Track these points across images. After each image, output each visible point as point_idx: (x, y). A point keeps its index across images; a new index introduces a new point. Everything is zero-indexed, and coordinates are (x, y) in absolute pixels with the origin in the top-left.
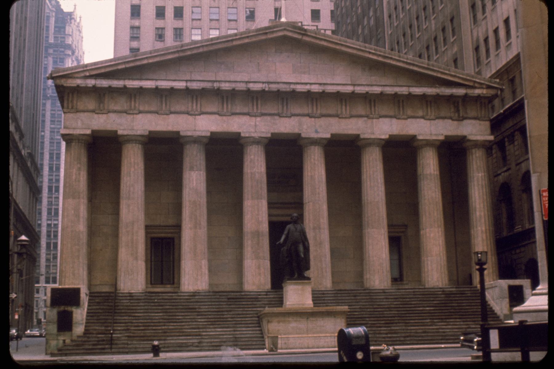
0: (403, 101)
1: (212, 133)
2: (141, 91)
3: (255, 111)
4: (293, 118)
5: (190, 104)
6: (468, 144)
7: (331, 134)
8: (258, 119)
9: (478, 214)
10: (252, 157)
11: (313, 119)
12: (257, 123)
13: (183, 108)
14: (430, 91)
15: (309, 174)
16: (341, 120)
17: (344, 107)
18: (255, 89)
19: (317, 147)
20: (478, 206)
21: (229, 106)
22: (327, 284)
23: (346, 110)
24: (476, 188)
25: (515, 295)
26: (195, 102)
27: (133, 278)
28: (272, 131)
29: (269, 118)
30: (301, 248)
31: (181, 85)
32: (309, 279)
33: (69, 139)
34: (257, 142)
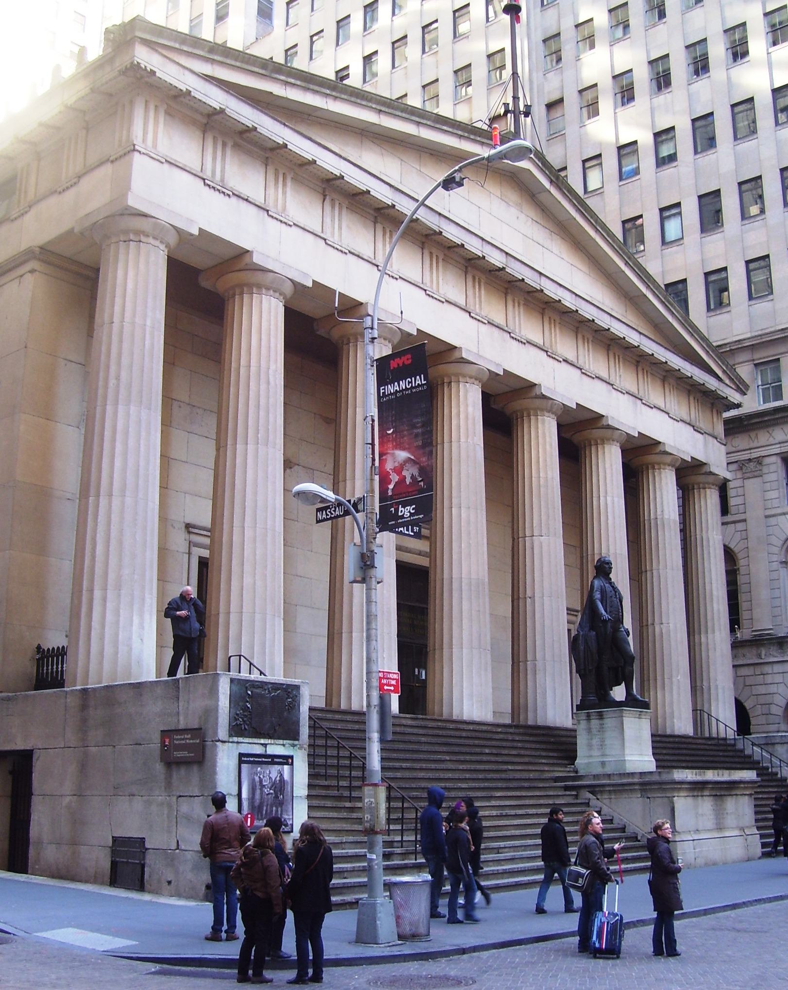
6: (701, 479)
8: (485, 329)
9: (715, 605)
16: (584, 377)
20: (715, 593)
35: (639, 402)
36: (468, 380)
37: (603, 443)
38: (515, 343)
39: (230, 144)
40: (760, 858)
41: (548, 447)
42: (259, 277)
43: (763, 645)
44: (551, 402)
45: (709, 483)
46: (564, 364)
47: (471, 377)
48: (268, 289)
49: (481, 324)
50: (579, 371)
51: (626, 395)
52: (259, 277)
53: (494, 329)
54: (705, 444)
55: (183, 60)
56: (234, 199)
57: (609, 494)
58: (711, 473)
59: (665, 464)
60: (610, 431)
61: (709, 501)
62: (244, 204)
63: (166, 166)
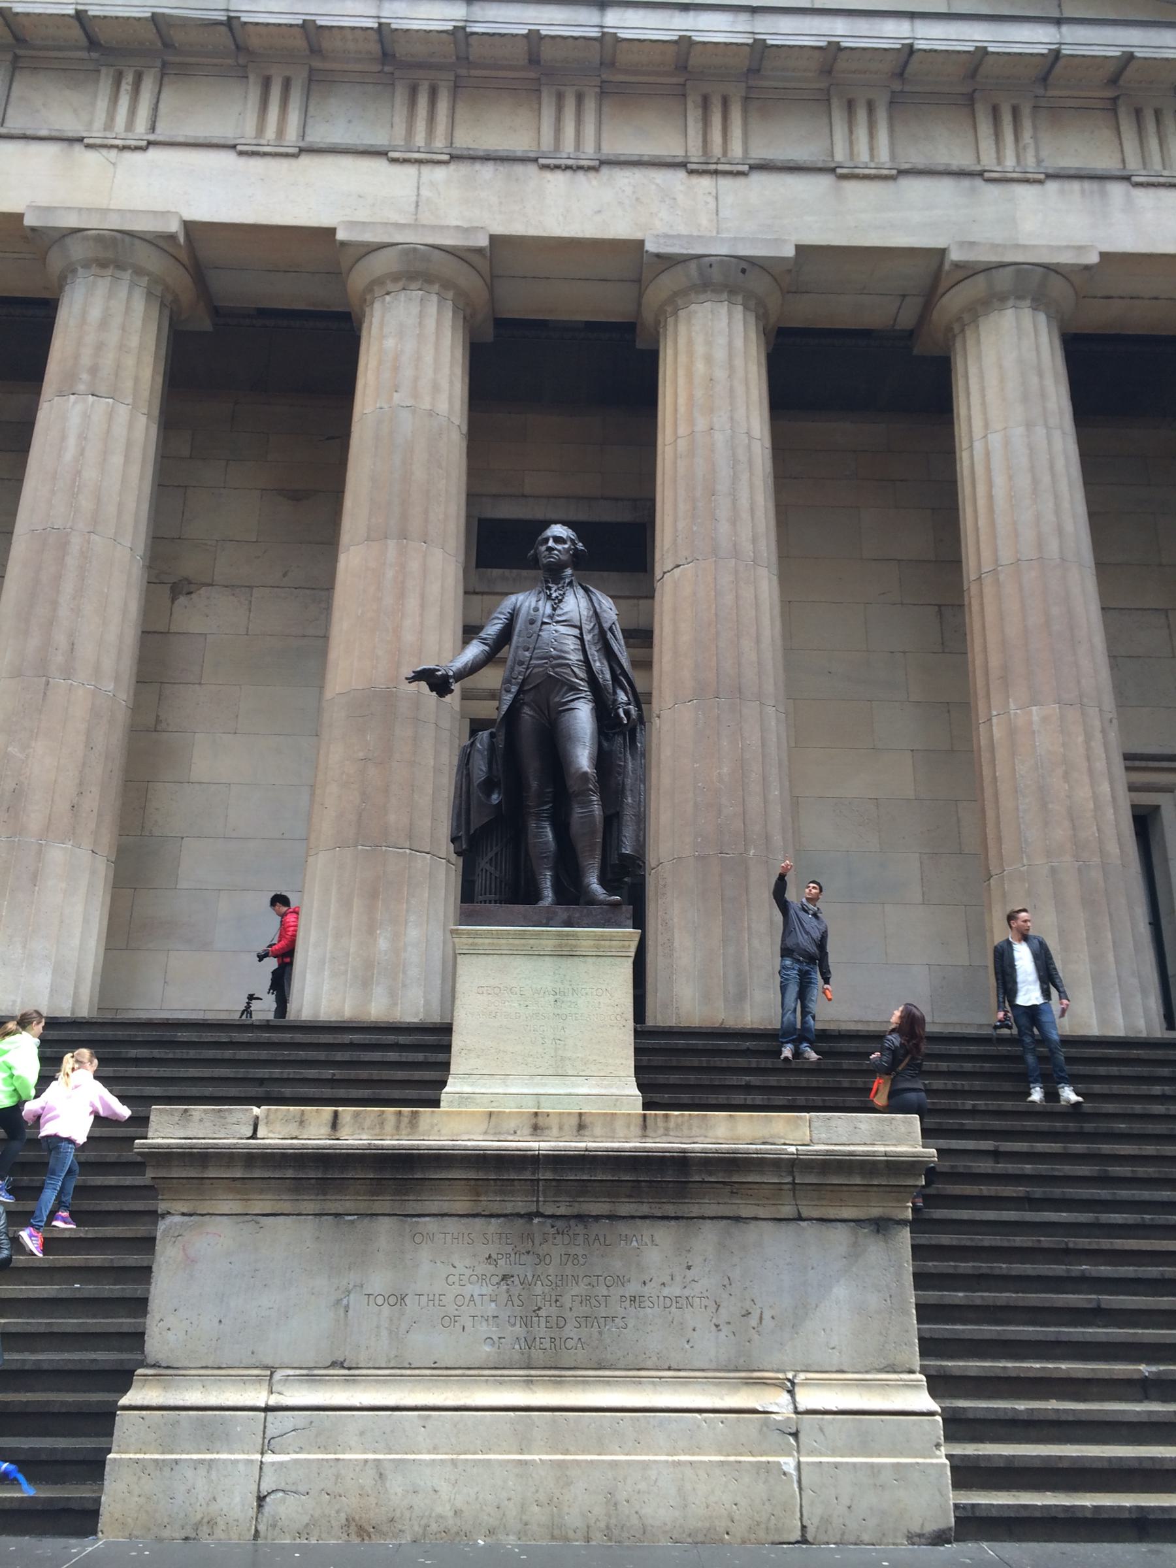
1: (188, 225)
3: (420, 139)
4: (605, 171)
5: (102, 104)
7: (799, 248)
10: (390, 343)
11: (706, 182)
12: (425, 192)
15: (682, 431)
16: (850, 186)
17: (862, 133)
18: (415, 25)
19: (723, 309)
21: (294, 118)
23: (872, 149)
28: (499, 229)
29: (487, 171)
35: (1117, 190)
36: (390, 286)
37: (975, 319)
38: (559, 178)
40: (940, 1538)
41: (700, 367)
44: (693, 265)
46: (757, 178)
47: (396, 277)
49: (426, 170)
51: (1052, 186)
53: (478, 166)
60: (981, 279)
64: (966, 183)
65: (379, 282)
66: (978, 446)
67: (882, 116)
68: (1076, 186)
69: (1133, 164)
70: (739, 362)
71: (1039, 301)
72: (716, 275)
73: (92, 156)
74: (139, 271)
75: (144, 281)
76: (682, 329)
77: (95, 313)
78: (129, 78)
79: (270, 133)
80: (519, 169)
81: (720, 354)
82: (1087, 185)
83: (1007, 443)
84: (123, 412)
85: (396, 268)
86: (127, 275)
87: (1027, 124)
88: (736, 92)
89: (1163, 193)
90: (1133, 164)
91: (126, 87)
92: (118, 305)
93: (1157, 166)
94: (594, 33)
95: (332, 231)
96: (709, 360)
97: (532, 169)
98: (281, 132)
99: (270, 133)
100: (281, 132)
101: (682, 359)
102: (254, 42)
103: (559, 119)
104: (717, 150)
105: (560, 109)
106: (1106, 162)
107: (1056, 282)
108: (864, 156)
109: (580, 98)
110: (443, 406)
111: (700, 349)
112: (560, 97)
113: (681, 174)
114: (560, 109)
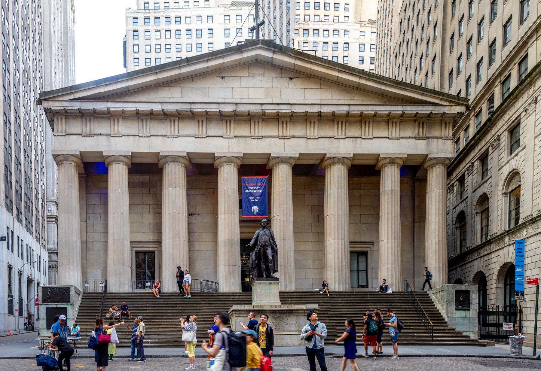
0: (369, 122)
2: (123, 116)
5: (169, 127)
10: (226, 175)
11: (282, 140)
13: (163, 132)
14: (398, 109)
16: (309, 140)
17: (312, 128)
22: (292, 288)
24: (433, 203)
25: (461, 299)
26: (172, 123)
27: (122, 282)
30: (269, 251)
31: (157, 108)
32: (277, 279)
33: (59, 159)
34: (229, 160)
35: (359, 140)
39: (92, 118)
41: (281, 178)
42: (110, 159)
43: (492, 243)
45: (434, 164)
46: (292, 139)
47: (226, 162)
48: (115, 161)
50: (305, 139)
51: (347, 139)
52: (110, 159)
53: (240, 138)
54: (428, 144)
55: (61, 99)
56: (95, 137)
57: (332, 188)
58: (432, 159)
59: (387, 164)
61: (434, 173)
62: (100, 137)
63: (67, 136)
64: (331, 139)
65: (223, 163)
66: (329, 191)
67: (316, 125)
68: (351, 139)
69: (363, 134)
70: (288, 177)
71: (343, 163)
72: (284, 160)
73: (168, 139)
74: (180, 162)
75: (181, 164)
76: (277, 170)
77: (173, 172)
78: (173, 122)
79: (200, 133)
80: (248, 139)
81: (285, 176)
82: (353, 139)
83: (334, 192)
84: (181, 190)
85: (226, 160)
86: (178, 163)
87: (344, 126)
88: (288, 120)
89: (367, 140)
90: (363, 134)
91: (172, 123)
92: (177, 170)
93: (367, 135)
94: (260, 111)
95: (214, 153)
96: (282, 177)
97: (250, 138)
98: (202, 132)
99: (200, 133)
100: (202, 132)
101: (277, 176)
102: (195, 113)
103: (254, 127)
104: (285, 134)
105: (255, 125)
106: (357, 134)
107: (346, 160)
108: (312, 135)
109: (258, 122)
110: (235, 187)
111: (281, 175)
112: (255, 122)
113: (278, 139)
114: (255, 125)
